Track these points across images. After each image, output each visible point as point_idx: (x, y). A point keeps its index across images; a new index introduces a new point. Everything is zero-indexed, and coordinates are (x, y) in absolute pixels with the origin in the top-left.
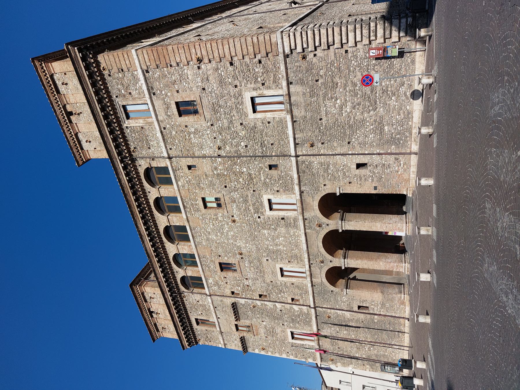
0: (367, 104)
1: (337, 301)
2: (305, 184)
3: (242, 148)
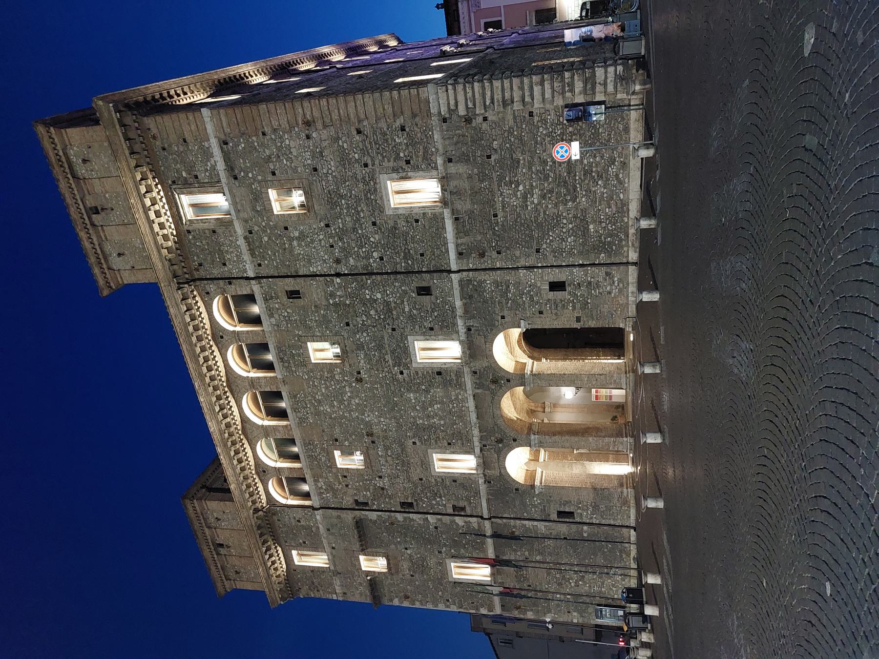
1: (523, 504)
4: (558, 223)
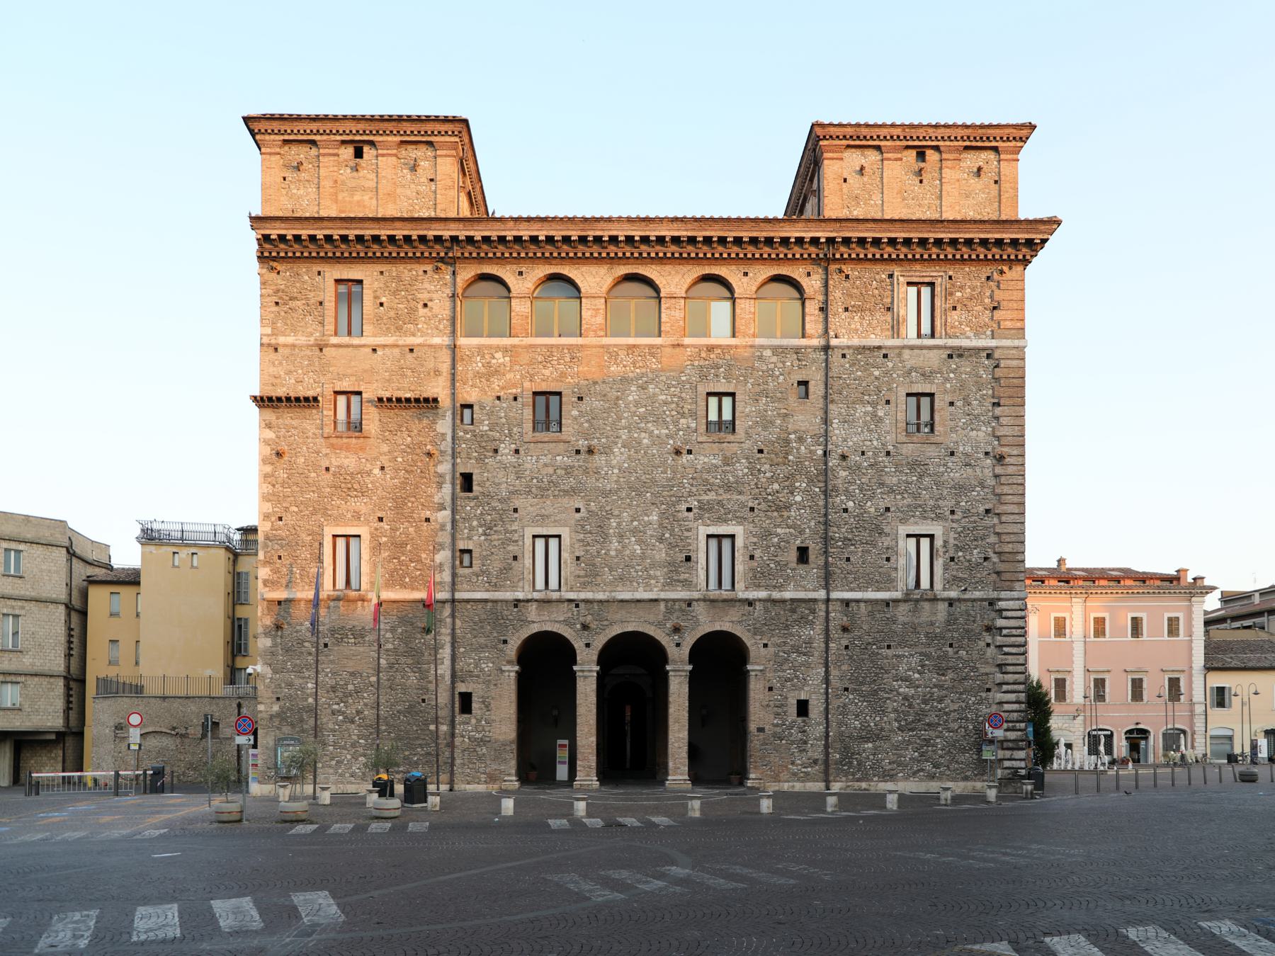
0: (911, 718)
2: (767, 610)
3: (842, 501)
4: (875, 711)
